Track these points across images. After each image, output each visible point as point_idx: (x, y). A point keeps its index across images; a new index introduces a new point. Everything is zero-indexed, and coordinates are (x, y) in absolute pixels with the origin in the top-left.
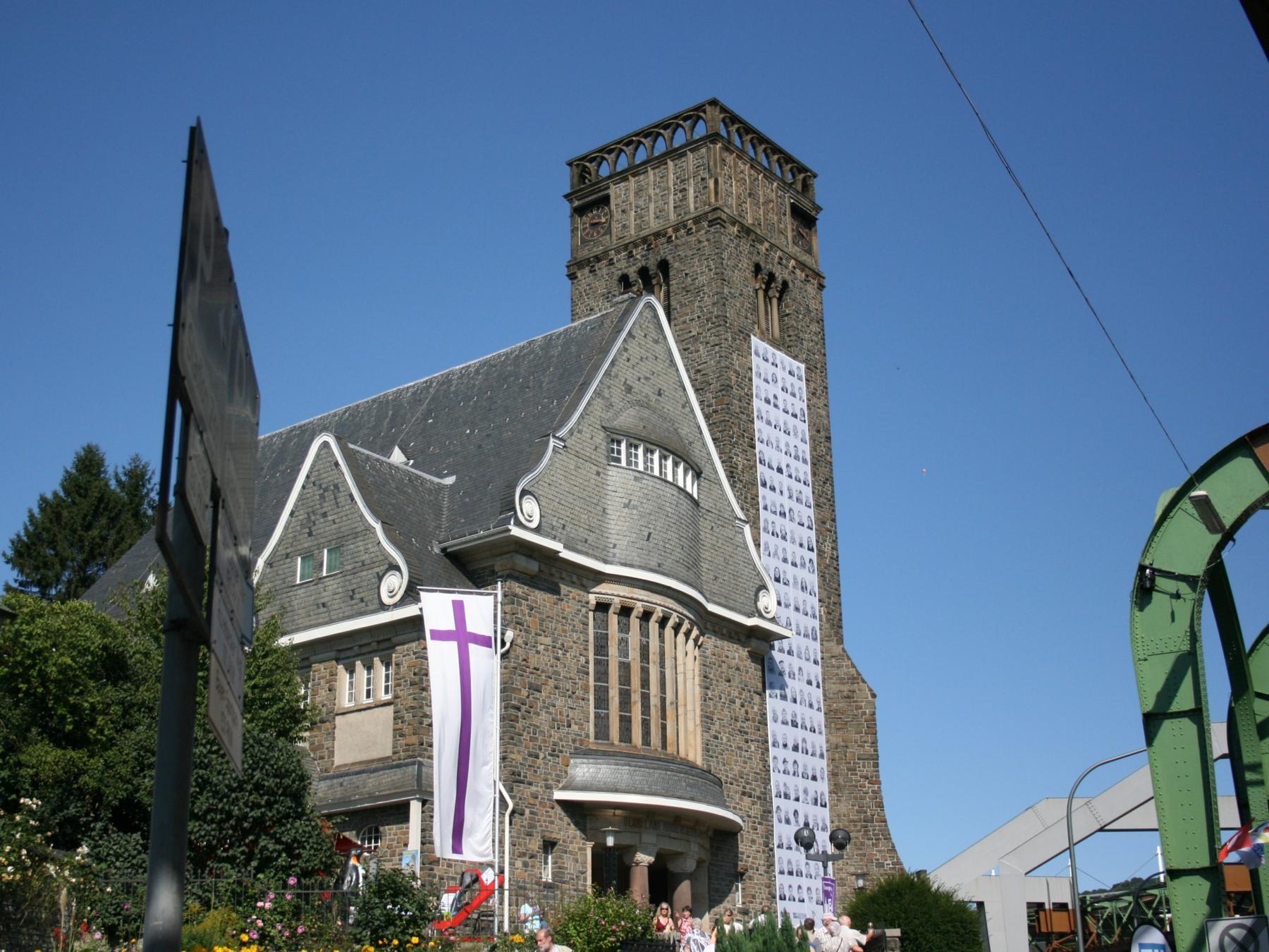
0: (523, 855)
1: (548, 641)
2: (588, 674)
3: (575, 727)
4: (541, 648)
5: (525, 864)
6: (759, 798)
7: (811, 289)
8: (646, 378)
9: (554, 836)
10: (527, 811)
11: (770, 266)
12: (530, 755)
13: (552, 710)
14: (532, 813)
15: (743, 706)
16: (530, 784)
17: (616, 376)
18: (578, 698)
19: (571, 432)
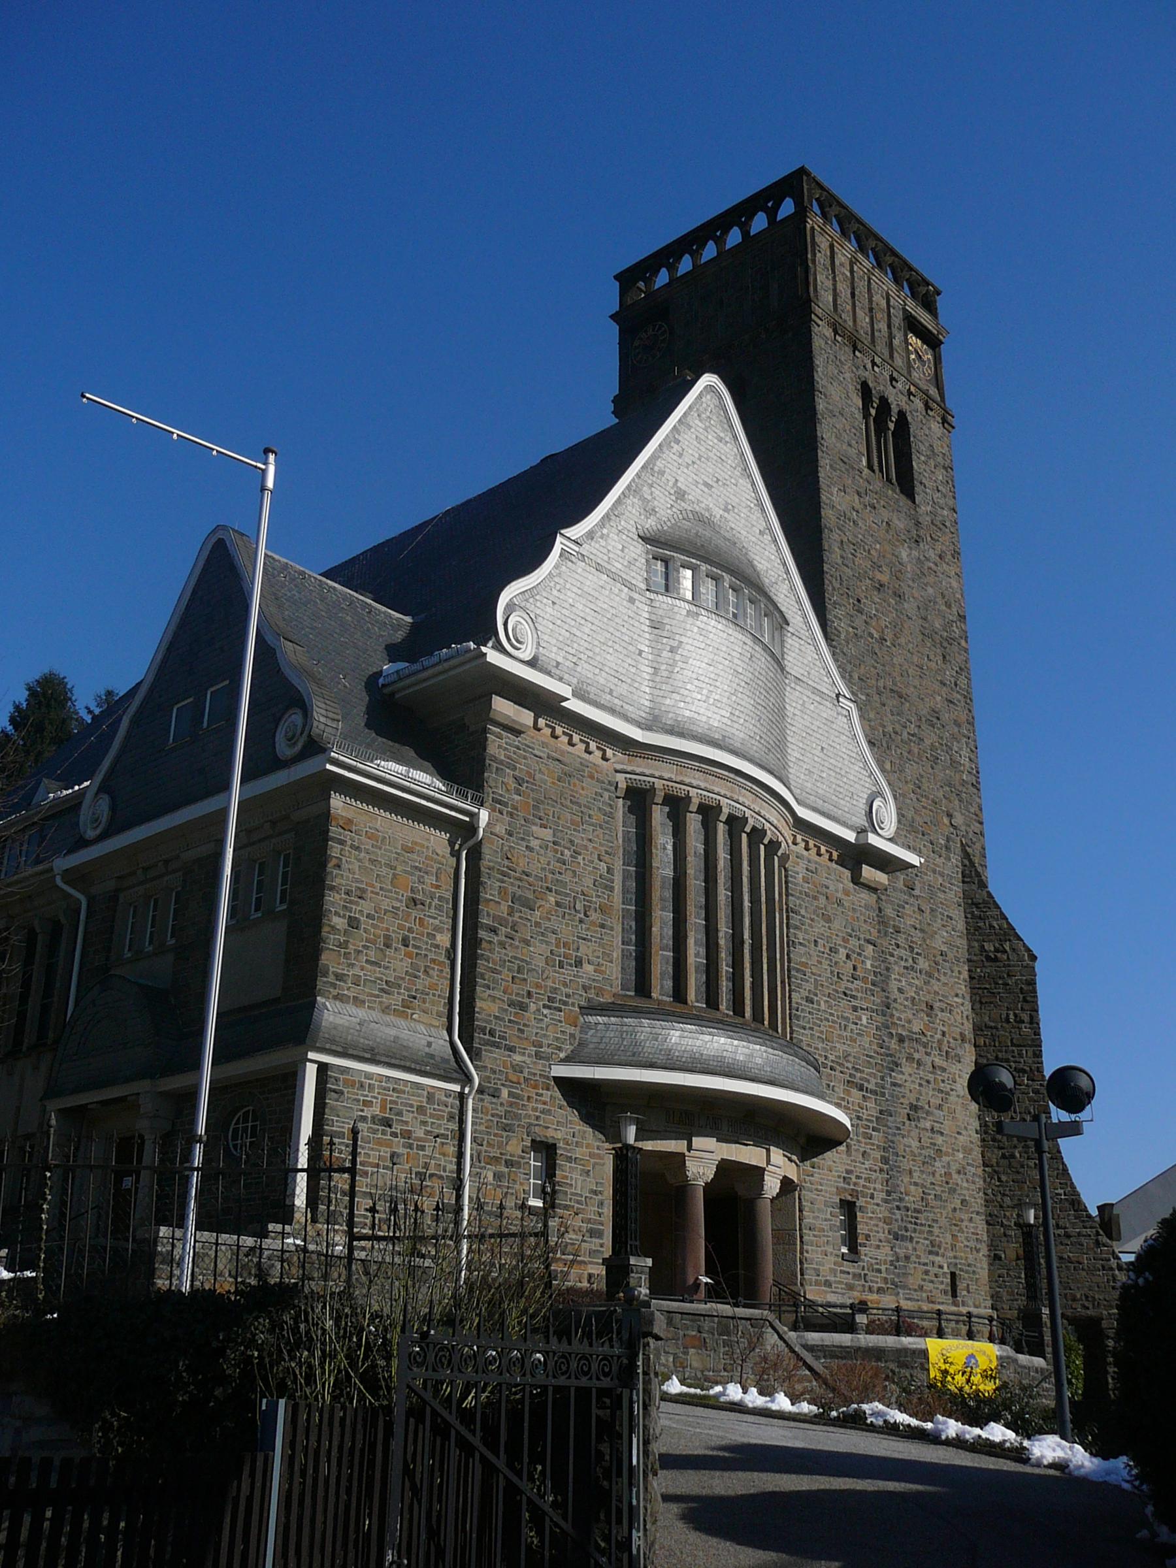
0: (495, 1160)
1: (547, 834)
2: (612, 889)
3: (589, 968)
4: (535, 843)
5: (498, 1176)
6: (874, 1092)
7: (936, 427)
8: (706, 484)
9: (550, 1133)
10: (505, 1093)
11: (882, 388)
12: (511, 1004)
13: (552, 938)
14: (510, 1094)
15: (848, 957)
16: (511, 1049)
17: (662, 473)
18: (593, 923)
19: (590, 535)
